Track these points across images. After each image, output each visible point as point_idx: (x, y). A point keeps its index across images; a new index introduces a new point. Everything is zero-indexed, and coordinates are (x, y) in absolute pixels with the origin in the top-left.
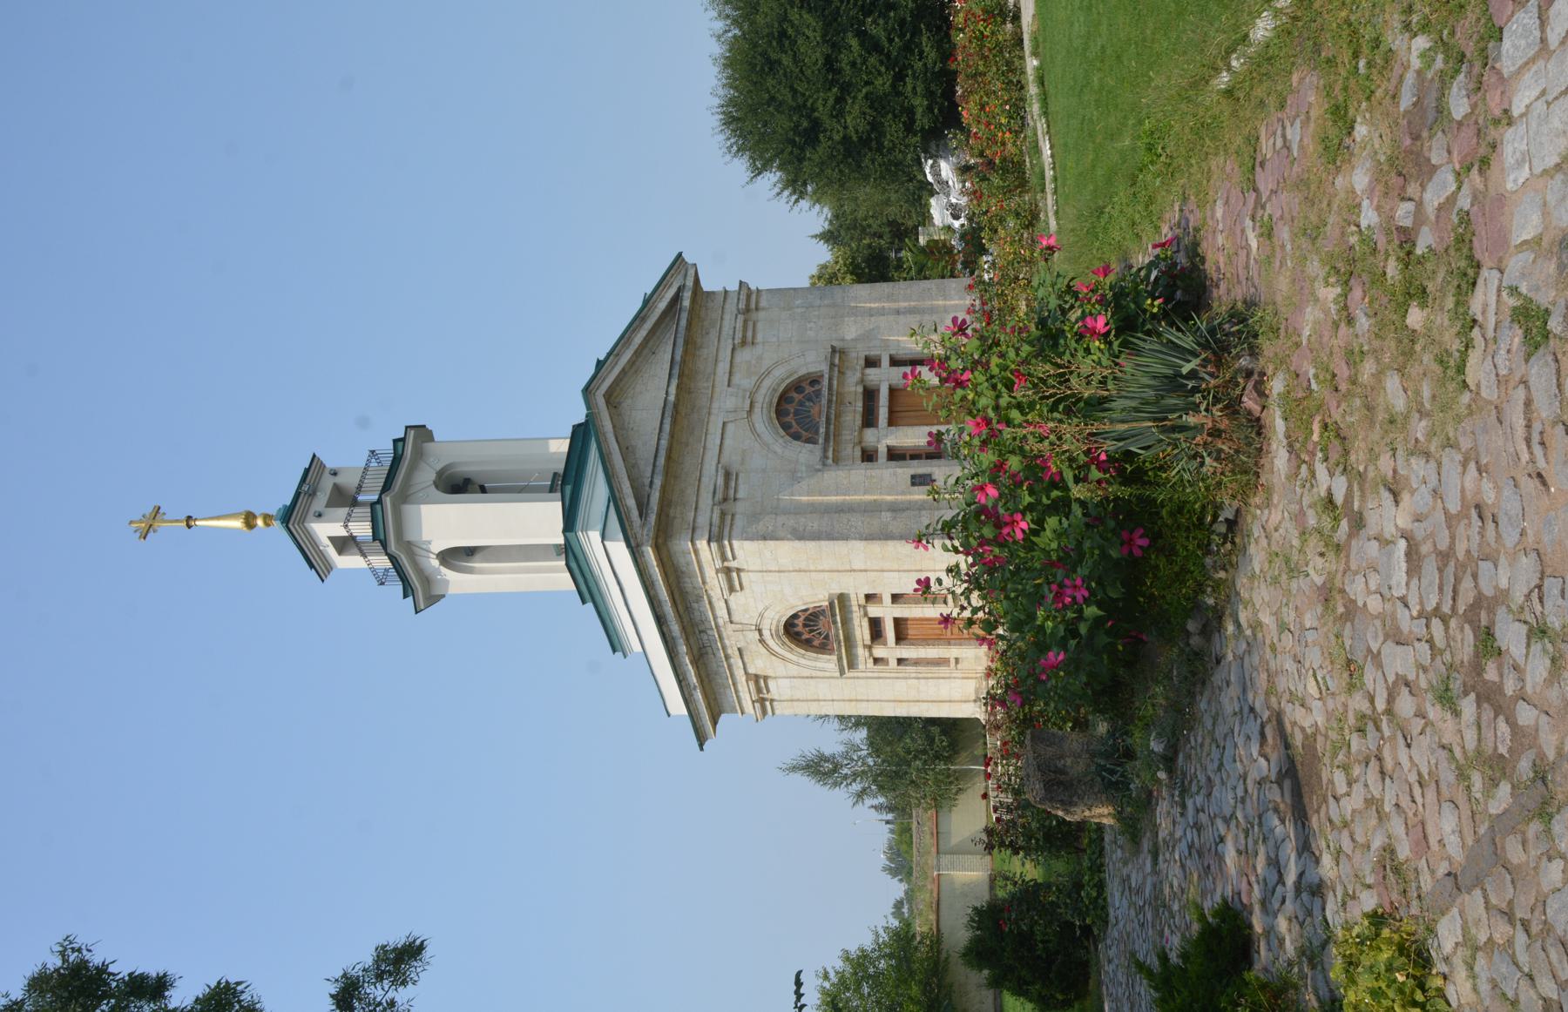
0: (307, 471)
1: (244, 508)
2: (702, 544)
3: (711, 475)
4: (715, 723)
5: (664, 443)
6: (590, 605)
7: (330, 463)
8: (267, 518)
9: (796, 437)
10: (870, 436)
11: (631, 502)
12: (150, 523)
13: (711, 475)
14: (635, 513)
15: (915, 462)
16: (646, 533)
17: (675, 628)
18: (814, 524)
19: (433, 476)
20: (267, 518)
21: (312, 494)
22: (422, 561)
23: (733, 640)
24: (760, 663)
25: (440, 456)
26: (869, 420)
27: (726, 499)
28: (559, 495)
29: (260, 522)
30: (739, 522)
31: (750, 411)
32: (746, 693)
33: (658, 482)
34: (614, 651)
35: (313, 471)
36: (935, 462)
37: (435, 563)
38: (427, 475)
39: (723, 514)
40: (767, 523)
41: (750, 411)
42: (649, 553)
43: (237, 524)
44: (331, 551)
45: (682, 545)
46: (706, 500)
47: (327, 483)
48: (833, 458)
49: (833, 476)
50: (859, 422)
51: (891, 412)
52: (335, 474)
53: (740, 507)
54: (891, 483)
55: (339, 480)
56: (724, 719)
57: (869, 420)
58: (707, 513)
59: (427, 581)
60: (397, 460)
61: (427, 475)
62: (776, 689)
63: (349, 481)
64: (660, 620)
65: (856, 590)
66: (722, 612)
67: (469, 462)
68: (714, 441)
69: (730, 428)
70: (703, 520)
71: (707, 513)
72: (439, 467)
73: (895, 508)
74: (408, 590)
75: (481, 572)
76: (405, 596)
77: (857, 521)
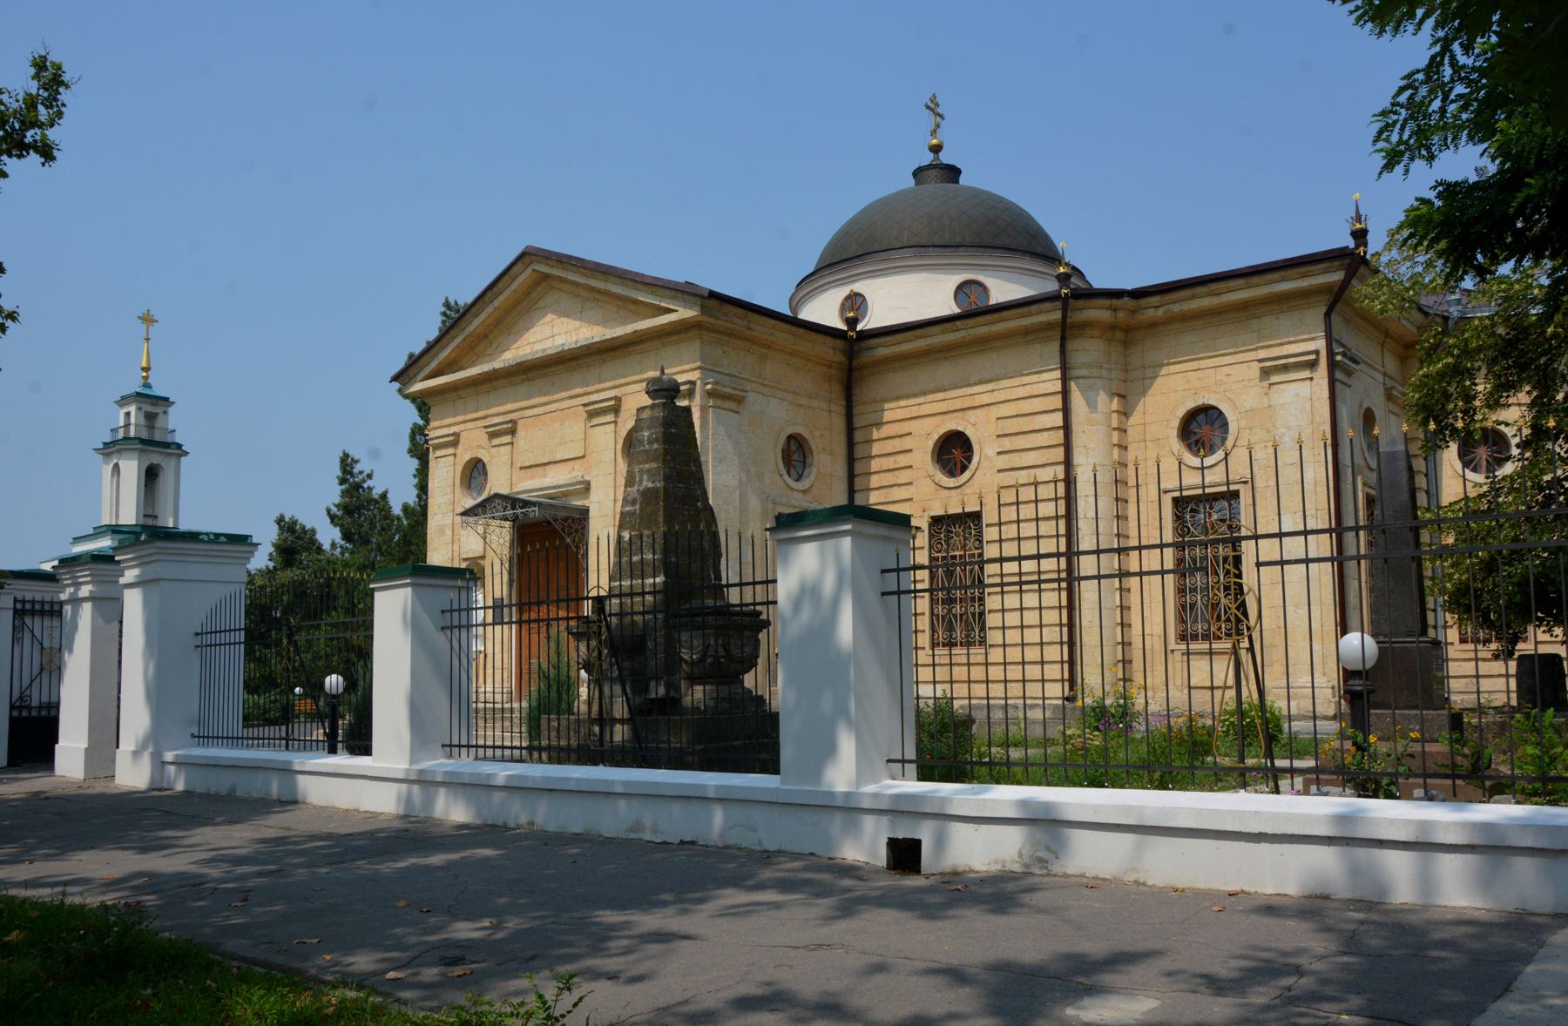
0: (166, 399)
6: (91, 532)
7: (171, 410)
8: (146, 378)
12: (148, 319)
19: (155, 462)
20: (146, 378)
21: (153, 404)
22: (115, 455)
25: (168, 465)
29: (144, 374)
34: (74, 539)
37: (115, 461)
38: (155, 459)
43: (144, 364)
44: (125, 410)
47: (159, 410)
52: (165, 412)
55: (161, 417)
60: (167, 445)
61: (155, 459)
63: (159, 423)
67: (165, 481)
72: (162, 464)
75: (112, 480)
76: (105, 444)
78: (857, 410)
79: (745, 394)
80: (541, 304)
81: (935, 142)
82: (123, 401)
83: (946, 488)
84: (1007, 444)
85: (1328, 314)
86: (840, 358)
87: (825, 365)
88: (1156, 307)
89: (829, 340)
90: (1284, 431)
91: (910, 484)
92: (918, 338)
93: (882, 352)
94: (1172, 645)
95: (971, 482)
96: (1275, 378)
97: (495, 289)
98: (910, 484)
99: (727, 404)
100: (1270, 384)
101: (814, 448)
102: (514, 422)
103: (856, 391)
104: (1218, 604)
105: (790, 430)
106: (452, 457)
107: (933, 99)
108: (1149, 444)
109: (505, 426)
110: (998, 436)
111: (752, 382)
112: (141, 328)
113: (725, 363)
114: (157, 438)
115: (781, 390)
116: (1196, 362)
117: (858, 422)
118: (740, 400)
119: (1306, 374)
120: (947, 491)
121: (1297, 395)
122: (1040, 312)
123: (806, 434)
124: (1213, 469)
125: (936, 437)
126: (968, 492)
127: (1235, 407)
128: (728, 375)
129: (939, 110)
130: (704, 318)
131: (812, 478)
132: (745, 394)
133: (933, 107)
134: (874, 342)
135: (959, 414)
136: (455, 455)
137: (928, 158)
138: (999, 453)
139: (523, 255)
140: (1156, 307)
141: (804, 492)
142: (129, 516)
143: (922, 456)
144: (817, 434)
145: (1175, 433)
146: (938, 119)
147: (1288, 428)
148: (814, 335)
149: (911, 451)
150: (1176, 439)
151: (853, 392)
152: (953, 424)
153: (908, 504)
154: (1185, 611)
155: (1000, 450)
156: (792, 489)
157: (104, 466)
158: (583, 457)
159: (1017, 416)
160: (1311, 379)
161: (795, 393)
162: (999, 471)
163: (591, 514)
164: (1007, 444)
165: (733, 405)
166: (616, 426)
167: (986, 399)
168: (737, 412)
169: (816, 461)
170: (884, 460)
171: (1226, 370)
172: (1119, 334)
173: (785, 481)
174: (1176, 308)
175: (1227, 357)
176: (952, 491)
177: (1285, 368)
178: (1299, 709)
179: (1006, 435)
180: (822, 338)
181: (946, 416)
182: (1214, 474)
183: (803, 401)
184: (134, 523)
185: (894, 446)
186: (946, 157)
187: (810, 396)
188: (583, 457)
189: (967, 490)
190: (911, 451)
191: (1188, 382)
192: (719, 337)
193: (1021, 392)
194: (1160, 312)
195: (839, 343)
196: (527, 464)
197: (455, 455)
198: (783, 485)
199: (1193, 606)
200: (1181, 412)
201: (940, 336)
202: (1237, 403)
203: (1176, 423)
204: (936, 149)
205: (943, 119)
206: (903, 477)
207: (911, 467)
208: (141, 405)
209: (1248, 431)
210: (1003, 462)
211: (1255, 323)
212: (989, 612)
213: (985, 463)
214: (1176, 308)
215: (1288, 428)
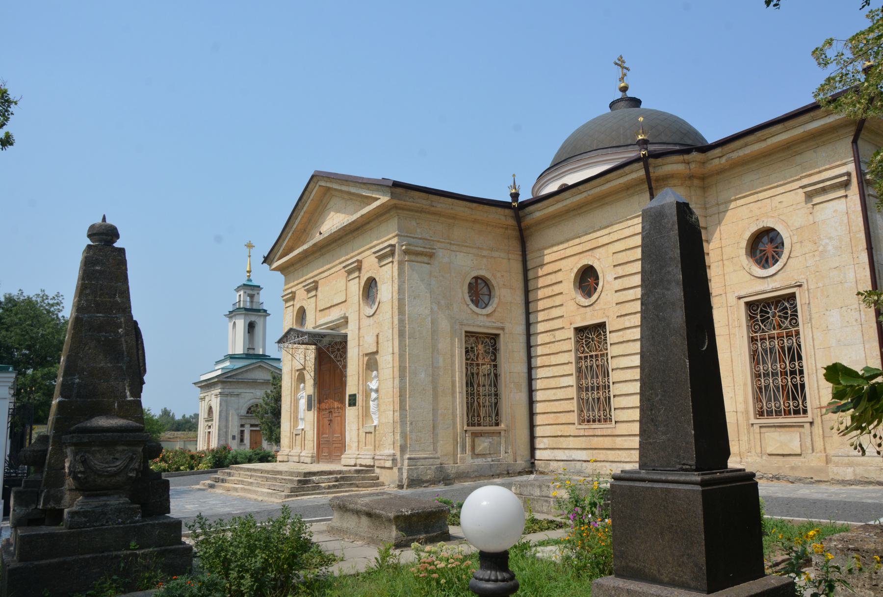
0: (259, 287)
1: (252, 270)
2: (220, 391)
3: (236, 391)
4: (199, 387)
5: (245, 380)
7: (261, 292)
9: (250, 409)
10: (249, 426)
11: (229, 375)
13: (236, 391)
14: (226, 376)
15: (239, 436)
16: (221, 379)
17: (208, 382)
18: (223, 414)
19: (253, 320)
21: (251, 290)
23: (209, 393)
24: (207, 399)
25: (259, 321)
26: (252, 426)
27: (231, 395)
28: (246, 352)
30: (224, 398)
31: (256, 398)
32: (202, 395)
33: (234, 380)
35: (258, 288)
36: (239, 440)
39: (227, 395)
40: (223, 403)
41: (256, 398)
42: (216, 380)
43: (248, 269)
44: (239, 294)
45: (220, 386)
46: (231, 390)
47: (255, 292)
48: (241, 417)
49: (236, 418)
50: (252, 423)
51: (255, 430)
52: (258, 294)
53: (229, 398)
54: (234, 430)
55: (256, 296)
56: (199, 389)
57: (252, 426)
58: (227, 391)
59: (231, 318)
60: (258, 311)
61: (253, 318)
62: (203, 402)
63: (255, 299)
64: (209, 379)
65: (214, 422)
66: (213, 392)
67: (258, 330)
68: (248, 391)
69: (252, 394)
70: (226, 390)
71: (227, 391)
73: (226, 433)
74: (230, 312)
76: (230, 312)
77: (224, 423)
78: (529, 257)
79: (434, 251)
80: (328, 207)
81: (622, 85)
82: (238, 289)
83: (586, 307)
84: (620, 271)
85: (855, 142)
86: (512, 222)
87: (502, 228)
88: (720, 157)
89: (499, 210)
90: (827, 241)
91: (562, 305)
92: (558, 202)
93: (538, 214)
94: (753, 421)
95: (598, 301)
96: (816, 200)
97: (303, 200)
98: (562, 305)
99: (419, 259)
100: (813, 205)
101: (495, 284)
102: (316, 282)
103: (528, 245)
104: (786, 385)
105: (474, 274)
106: (292, 307)
107: (621, 58)
108: (725, 262)
109: (311, 285)
110: (614, 266)
111: (441, 242)
112: (247, 250)
113: (418, 230)
114: (254, 307)
115: (467, 247)
117: (530, 265)
118: (431, 256)
119: (842, 193)
120: (584, 309)
122: (632, 172)
123: (488, 275)
124: (774, 278)
125: (576, 270)
126: (597, 308)
127: (788, 227)
128: (420, 239)
129: (625, 65)
130: (395, 201)
131: (495, 306)
132: (434, 251)
133: (620, 63)
134: (532, 208)
135: (590, 253)
136: (293, 305)
137: (619, 95)
138: (616, 278)
139: (313, 177)
140: (720, 157)
141: (488, 315)
142: (239, 350)
143: (568, 285)
144: (499, 275)
145: (743, 252)
146: (625, 71)
147: (830, 238)
148: (481, 207)
149: (561, 282)
150: (744, 257)
151: (527, 245)
152: (586, 260)
153: (560, 320)
154: (761, 392)
155: (616, 276)
156: (477, 314)
157: (229, 324)
158: (346, 301)
159: (626, 250)
160: (846, 196)
161: (478, 248)
162: (616, 291)
163: (349, 338)
164: (620, 271)
165: (426, 259)
166: (359, 279)
167: (605, 240)
168: (428, 264)
169: (497, 293)
170: (546, 290)
171: (779, 198)
172: (696, 182)
173: (471, 309)
174: (734, 155)
175: (779, 189)
176: (588, 308)
177: (824, 190)
178: (855, 475)
179: (619, 265)
180: (493, 209)
181: (582, 255)
182: (776, 281)
183: (485, 253)
184: (242, 353)
185: (551, 280)
186: (630, 94)
187: (492, 250)
188: (346, 301)
189: (596, 307)
190: (561, 282)
191: (751, 211)
192: (412, 213)
194: (723, 160)
195: (507, 211)
196: (322, 308)
197: (293, 305)
198: (469, 311)
199: (767, 387)
200: (747, 235)
201: (571, 199)
202: (789, 224)
203: (744, 244)
204: (624, 89)
205: (629, 70)
206: (557, 301)
207: (562, 293)
208: (246, 291)
209: (799, 245)
210: (619, 284)
211: (798, 159)
212: (614, 396)
213: (607, 286)
214: (734, 155)
215: (830, 238)
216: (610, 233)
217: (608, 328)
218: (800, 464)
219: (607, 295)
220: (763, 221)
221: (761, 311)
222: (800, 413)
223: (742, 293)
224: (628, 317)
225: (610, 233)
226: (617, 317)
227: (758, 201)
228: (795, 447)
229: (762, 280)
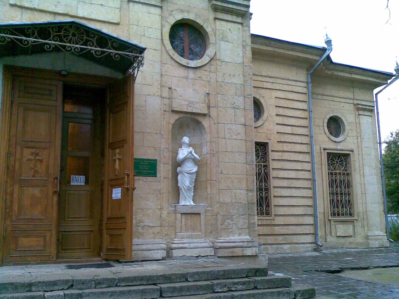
84: (281, 111)
95: (262, 126)
110: (276, 106)
116: (333, 98)
121: (367, 121)
126: (261, 131)
158: (118, 24)
162: (277, 124)
164: (281, 111)
167: (269, 86)
171: (343, 104)
175: (343, 99)
178: (379, 245)
191: (330, 105)
193: (290, 88)
210: (279, 120)
216: (273, 83)
217: (270, 148)
218: (352, 241)
219: (270, 124)
220: (336, 113)
221: (331, 159)
222: (344, 215)
223: (326, 147)
224: (285, 144)
225: (273, 83)
226: (278, 142)
227: (334, 101)
228: (351, 232)
229: (334, 143)
